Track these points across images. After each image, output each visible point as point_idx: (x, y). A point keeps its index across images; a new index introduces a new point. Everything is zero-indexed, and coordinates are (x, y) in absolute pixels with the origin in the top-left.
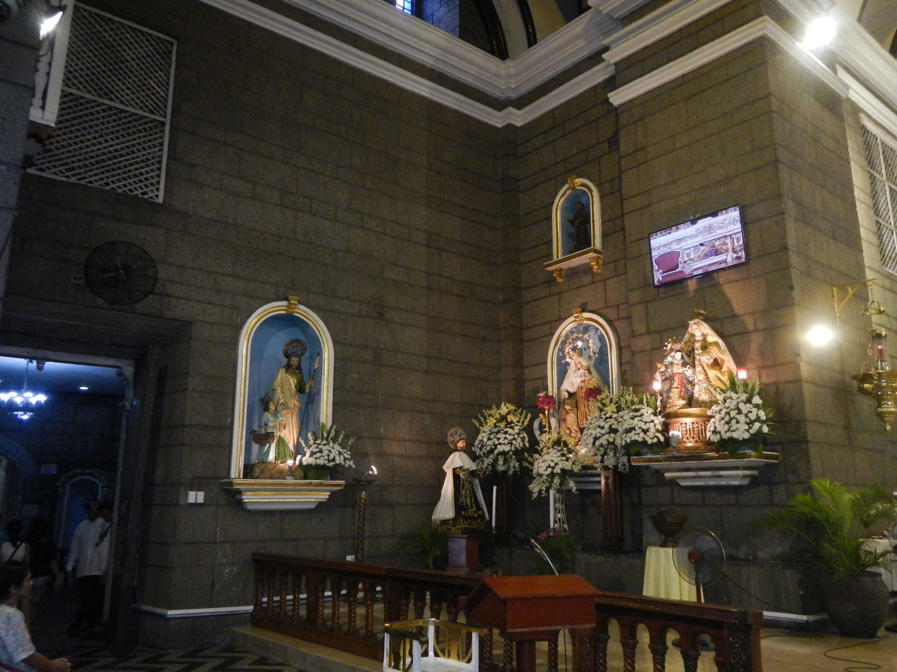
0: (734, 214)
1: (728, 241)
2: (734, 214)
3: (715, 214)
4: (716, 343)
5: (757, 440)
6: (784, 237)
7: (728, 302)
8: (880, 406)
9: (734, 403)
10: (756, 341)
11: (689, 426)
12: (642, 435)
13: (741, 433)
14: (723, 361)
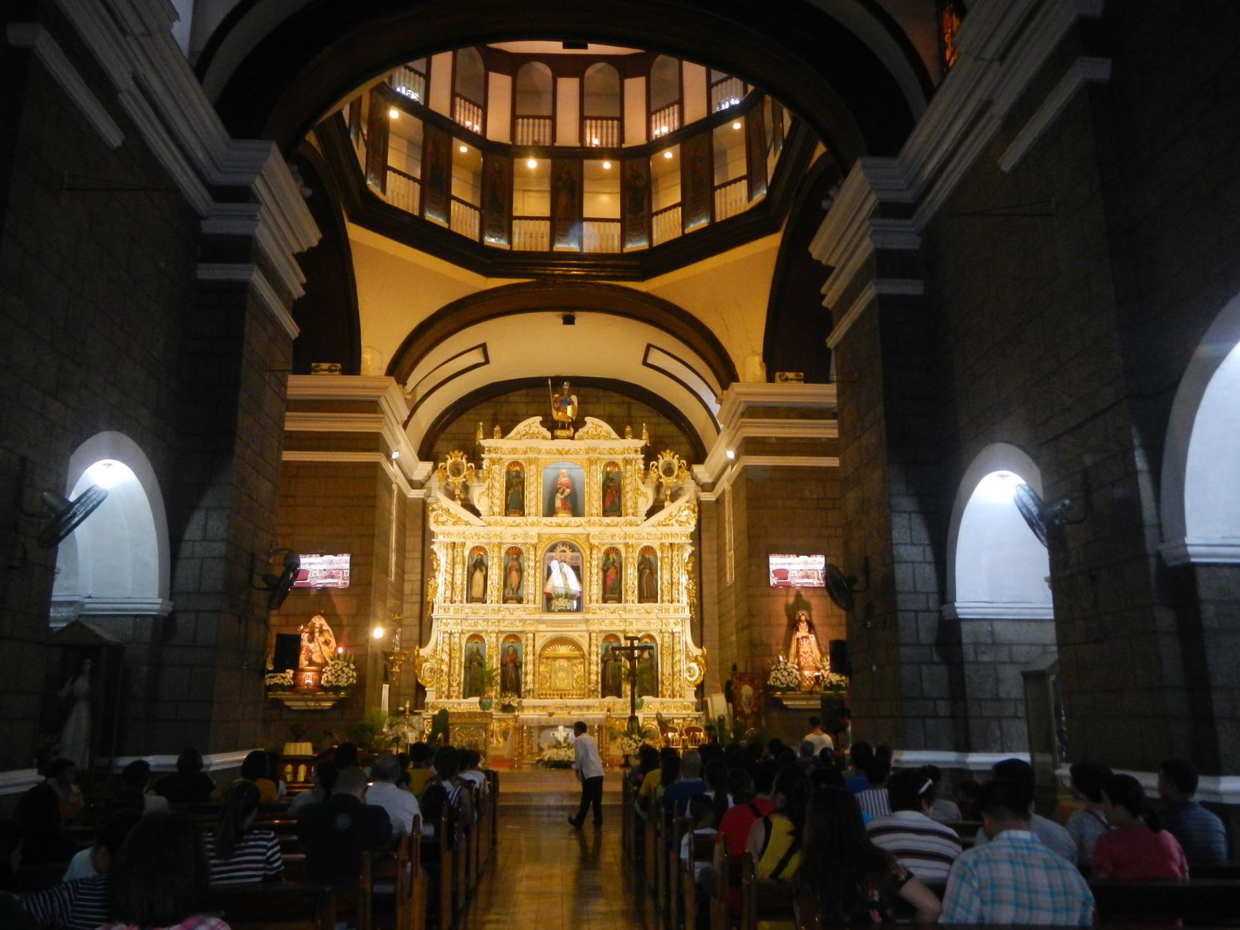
0: (346, 558)
1: (341, 572)
2: (346, 558)
3: (335, 555)
4: (328, 631)
5: (350, 686)
6: (371, 577)
7: (334, 606)
8: (392, 668)
9: (340, 667)
10: (346, 631)
11: (311, 677)
12: (282, 680)
13: (343, 682)
14: (330, 641)
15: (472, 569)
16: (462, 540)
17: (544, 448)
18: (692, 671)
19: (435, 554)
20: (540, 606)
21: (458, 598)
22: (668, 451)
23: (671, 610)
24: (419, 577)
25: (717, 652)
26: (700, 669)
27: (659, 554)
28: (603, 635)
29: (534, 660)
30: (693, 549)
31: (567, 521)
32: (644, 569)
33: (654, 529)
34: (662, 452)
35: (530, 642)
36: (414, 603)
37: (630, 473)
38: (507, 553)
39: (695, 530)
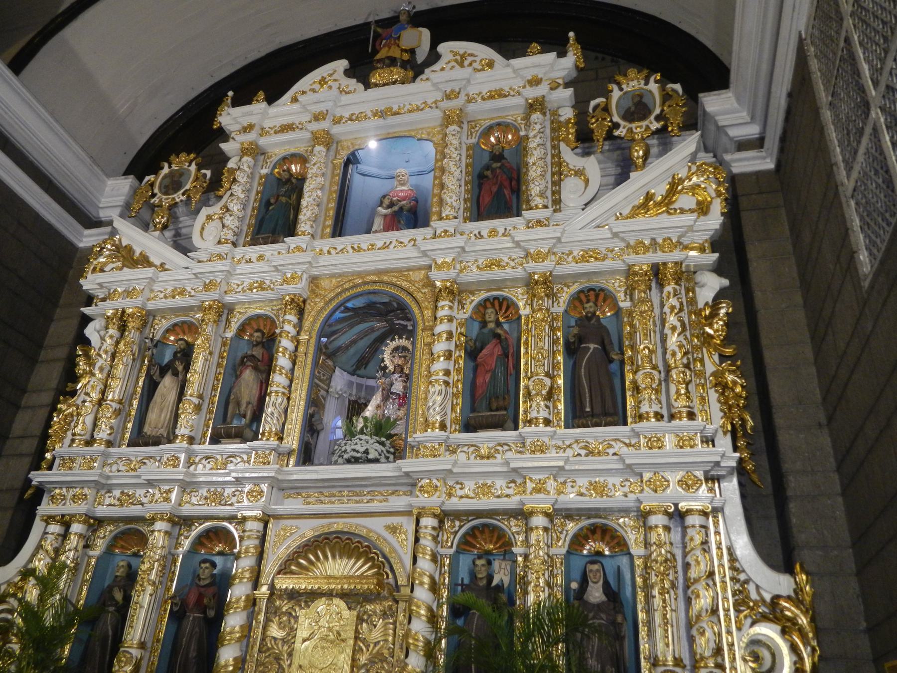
15: (155, 372)
16: (138, 301)
17: (347, 115)
18: (765, 654)
19: (87, 342)
20: (295, 446)
21: (103, 433)
22: (632, 72)
23: (669, 442)
24: (46, 398)
25: (853, 585)
26: (794, 648)
27: (625, 304)
28: (459, 529)
29: (253, 602)
30: (726, 282)
31: (380, 244)
32: (581, 339)
33: (605, 233)
34: (620, 78)
35: (251, 544)
36: (21, 455)
37: (538, 127)
38: (242, 330)
39: (723, 225)
